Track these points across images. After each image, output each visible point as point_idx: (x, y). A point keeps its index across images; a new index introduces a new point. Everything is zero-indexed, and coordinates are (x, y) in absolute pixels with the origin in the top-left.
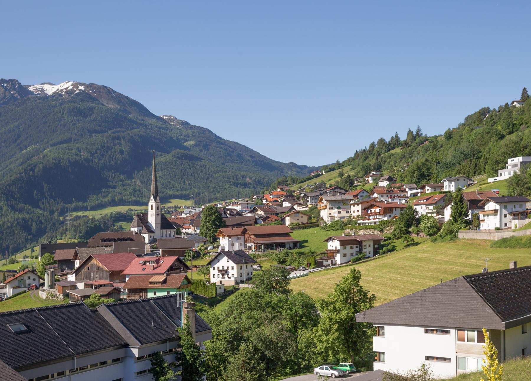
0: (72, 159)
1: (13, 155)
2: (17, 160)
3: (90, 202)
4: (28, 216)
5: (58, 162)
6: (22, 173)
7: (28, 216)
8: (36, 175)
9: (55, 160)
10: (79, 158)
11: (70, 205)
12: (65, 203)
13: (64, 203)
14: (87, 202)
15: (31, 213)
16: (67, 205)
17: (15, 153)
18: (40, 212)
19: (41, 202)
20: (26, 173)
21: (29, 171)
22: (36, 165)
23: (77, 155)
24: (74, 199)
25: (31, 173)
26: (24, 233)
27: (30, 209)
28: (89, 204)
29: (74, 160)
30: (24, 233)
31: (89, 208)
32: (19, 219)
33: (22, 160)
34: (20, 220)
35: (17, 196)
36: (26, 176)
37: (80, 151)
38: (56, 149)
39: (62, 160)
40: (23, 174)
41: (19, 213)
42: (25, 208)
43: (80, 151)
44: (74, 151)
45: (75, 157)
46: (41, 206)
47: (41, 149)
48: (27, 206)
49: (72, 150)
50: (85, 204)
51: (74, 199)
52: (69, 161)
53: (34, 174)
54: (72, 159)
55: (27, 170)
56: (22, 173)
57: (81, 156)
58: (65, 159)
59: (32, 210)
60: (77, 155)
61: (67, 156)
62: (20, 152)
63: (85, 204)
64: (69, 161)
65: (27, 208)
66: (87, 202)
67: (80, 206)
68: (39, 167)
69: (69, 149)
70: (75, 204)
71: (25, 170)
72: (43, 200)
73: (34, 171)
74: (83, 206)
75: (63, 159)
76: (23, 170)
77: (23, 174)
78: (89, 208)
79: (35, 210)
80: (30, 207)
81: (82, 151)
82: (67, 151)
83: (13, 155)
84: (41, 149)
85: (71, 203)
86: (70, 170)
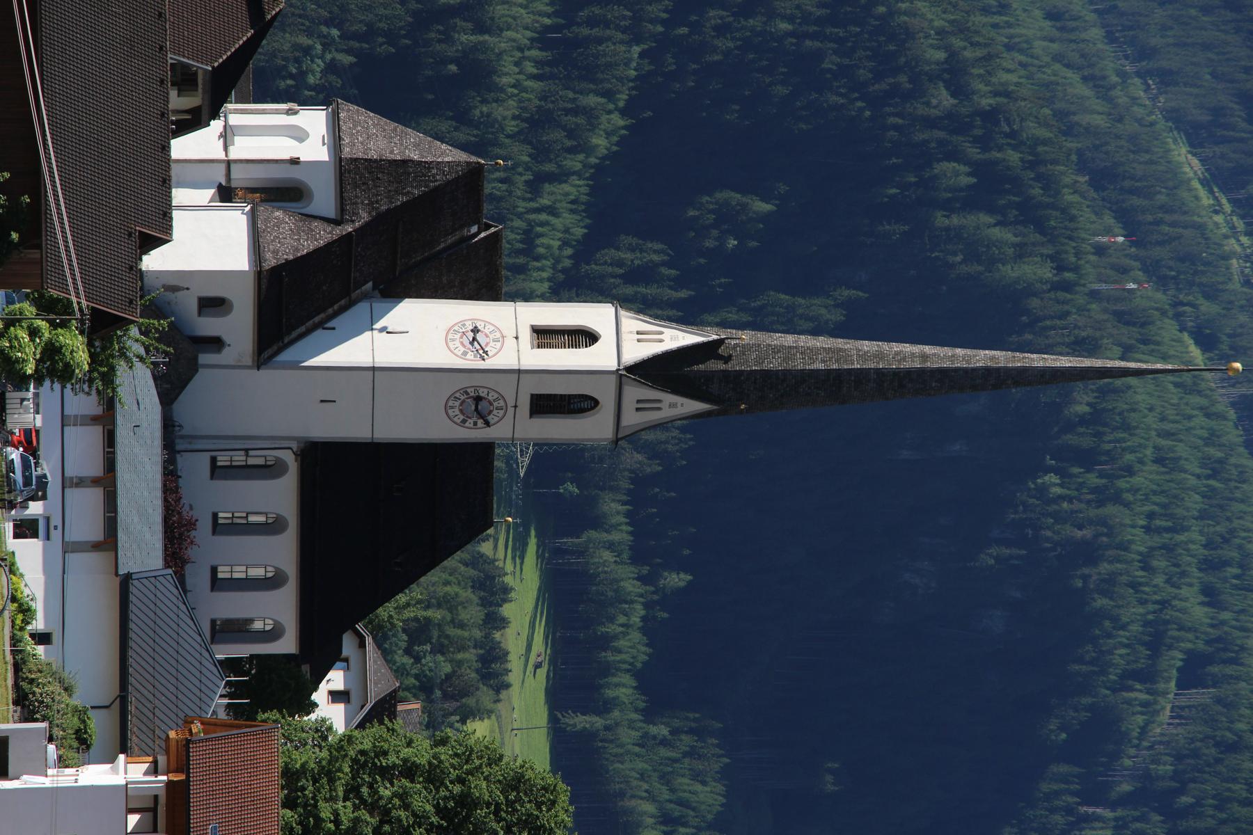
0: (1108, 585)
1: (1145, 53)
2: (1094, 80)
3: (645, 741)
4: (505, 112)
5: (1081, 439)
6: (959, 90)
7: (505, 112)
8: (941, 220)
9: (1096, 418)
10: (1119, 657)
11: (622, 535)
12: (637, 498)
13: (640, 482)
14: (650, 715)
15: (541, 153)
16: (613, 507)
17: (1166, 79)
18: (550, 241)
19: (654, 252)
20: (954, 123)
21: (974, 152)
22: (1041, 227)
23: (1156, 641)
24: (676, 580)
25: (955, 174)
26: (332, 68)
27: (583, 148)
28: (628, 736)
29: (1101, 602)
30: (332, 68)
31: (580, 721)
32: (481, 28)
33: (1099, 121)
34: (467, 38)
35: (721, 30)
36: (930, 123)
37: (1191, 676)
38: (1212, 438)
39: (1093, 479)
40: (943, 99)
41: (543, 39)
42: (592, 100)
43: (1191, 676)
44: (1199, 613)
45: (1133, 613)
46: (610, 254)
47: (1208, 308)
48: (618, 121)
49: (1211, 596)
50: (623, 689)
51: (676, 580)
52: (1088, 553)
53: (948, 207)
54: (1108, 585)
55: (984, 143)
56: (959, 90)
57: (1147, 676)
58: (1110, 510)
59: (574, 162)
60: (1156, 641)
61: (1140, 542)
62: (1176, 118)
63: (623, 689)
64: (1088, 553)
65: (590, 115)
66: (650, 715)
67: (605, 642)
68: (1021, 252)
69: (1209, 565)
70: (631, 587)
71: (991, 116)
72: (678, 283)
73: (971, 201)
74: (607, 670)
75: (1104, 496)
76: (986, 102)
77: (943, 99)
78: (580, 721)
79: (575, 188)
80: (600, 142)
81: (1201, 696)
82: (1194, 538)
83: (1145, 53)
84: (1208, 308)
85: (638, 555)
86: (988, 558)
